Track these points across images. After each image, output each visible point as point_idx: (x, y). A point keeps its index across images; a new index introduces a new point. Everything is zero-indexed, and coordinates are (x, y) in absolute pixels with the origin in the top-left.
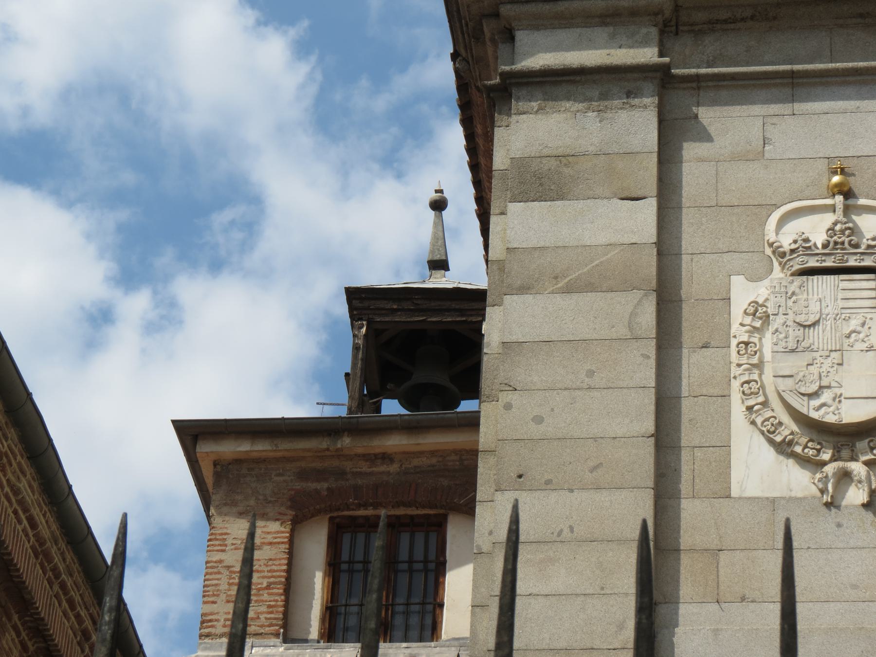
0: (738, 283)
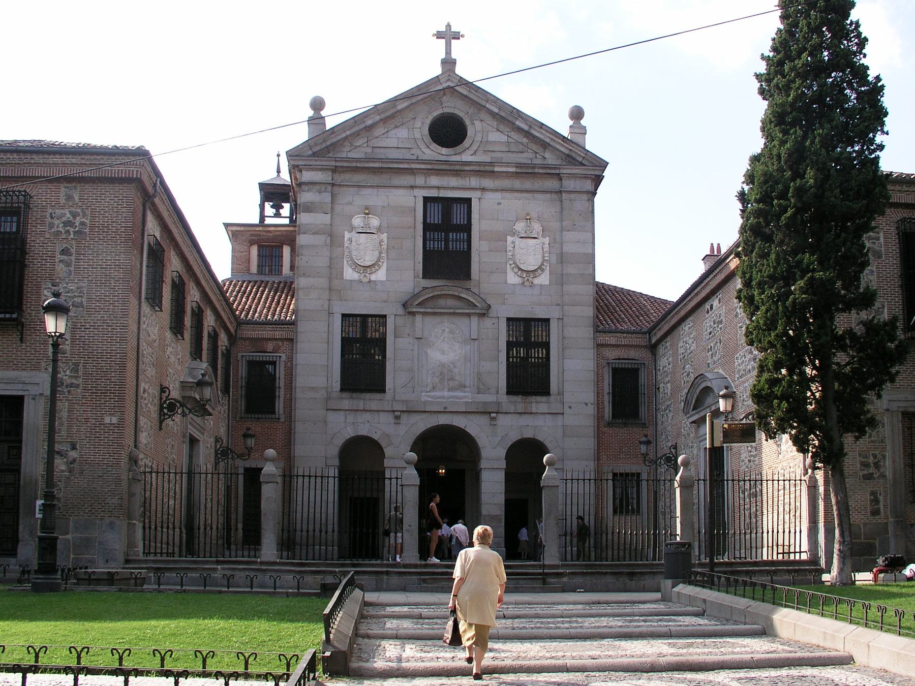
0: (346, 232)
